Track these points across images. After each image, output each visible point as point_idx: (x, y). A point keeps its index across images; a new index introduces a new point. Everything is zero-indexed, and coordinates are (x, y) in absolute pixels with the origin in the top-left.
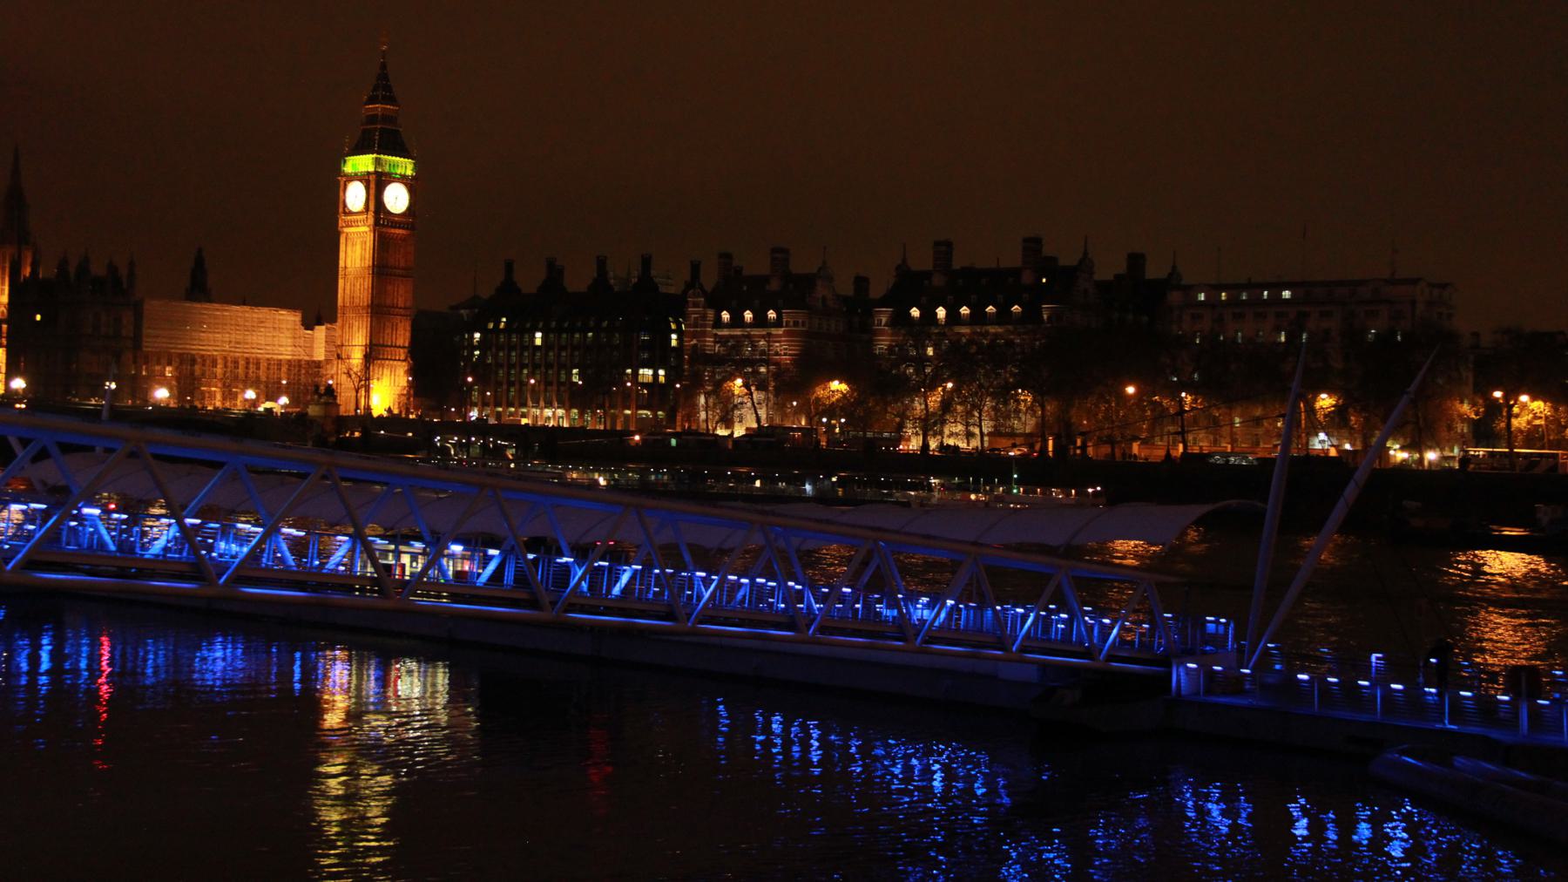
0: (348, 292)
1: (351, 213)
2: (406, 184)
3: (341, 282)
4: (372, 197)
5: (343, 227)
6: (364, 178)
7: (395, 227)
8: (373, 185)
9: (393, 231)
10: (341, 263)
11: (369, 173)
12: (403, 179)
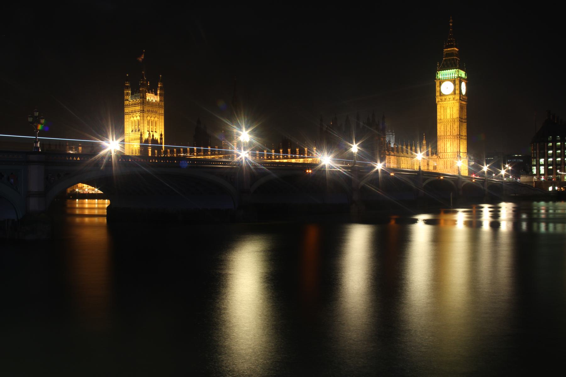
1: (444, 95)
3: (438, 126)
8: (457, 82)
10: (438, 117)
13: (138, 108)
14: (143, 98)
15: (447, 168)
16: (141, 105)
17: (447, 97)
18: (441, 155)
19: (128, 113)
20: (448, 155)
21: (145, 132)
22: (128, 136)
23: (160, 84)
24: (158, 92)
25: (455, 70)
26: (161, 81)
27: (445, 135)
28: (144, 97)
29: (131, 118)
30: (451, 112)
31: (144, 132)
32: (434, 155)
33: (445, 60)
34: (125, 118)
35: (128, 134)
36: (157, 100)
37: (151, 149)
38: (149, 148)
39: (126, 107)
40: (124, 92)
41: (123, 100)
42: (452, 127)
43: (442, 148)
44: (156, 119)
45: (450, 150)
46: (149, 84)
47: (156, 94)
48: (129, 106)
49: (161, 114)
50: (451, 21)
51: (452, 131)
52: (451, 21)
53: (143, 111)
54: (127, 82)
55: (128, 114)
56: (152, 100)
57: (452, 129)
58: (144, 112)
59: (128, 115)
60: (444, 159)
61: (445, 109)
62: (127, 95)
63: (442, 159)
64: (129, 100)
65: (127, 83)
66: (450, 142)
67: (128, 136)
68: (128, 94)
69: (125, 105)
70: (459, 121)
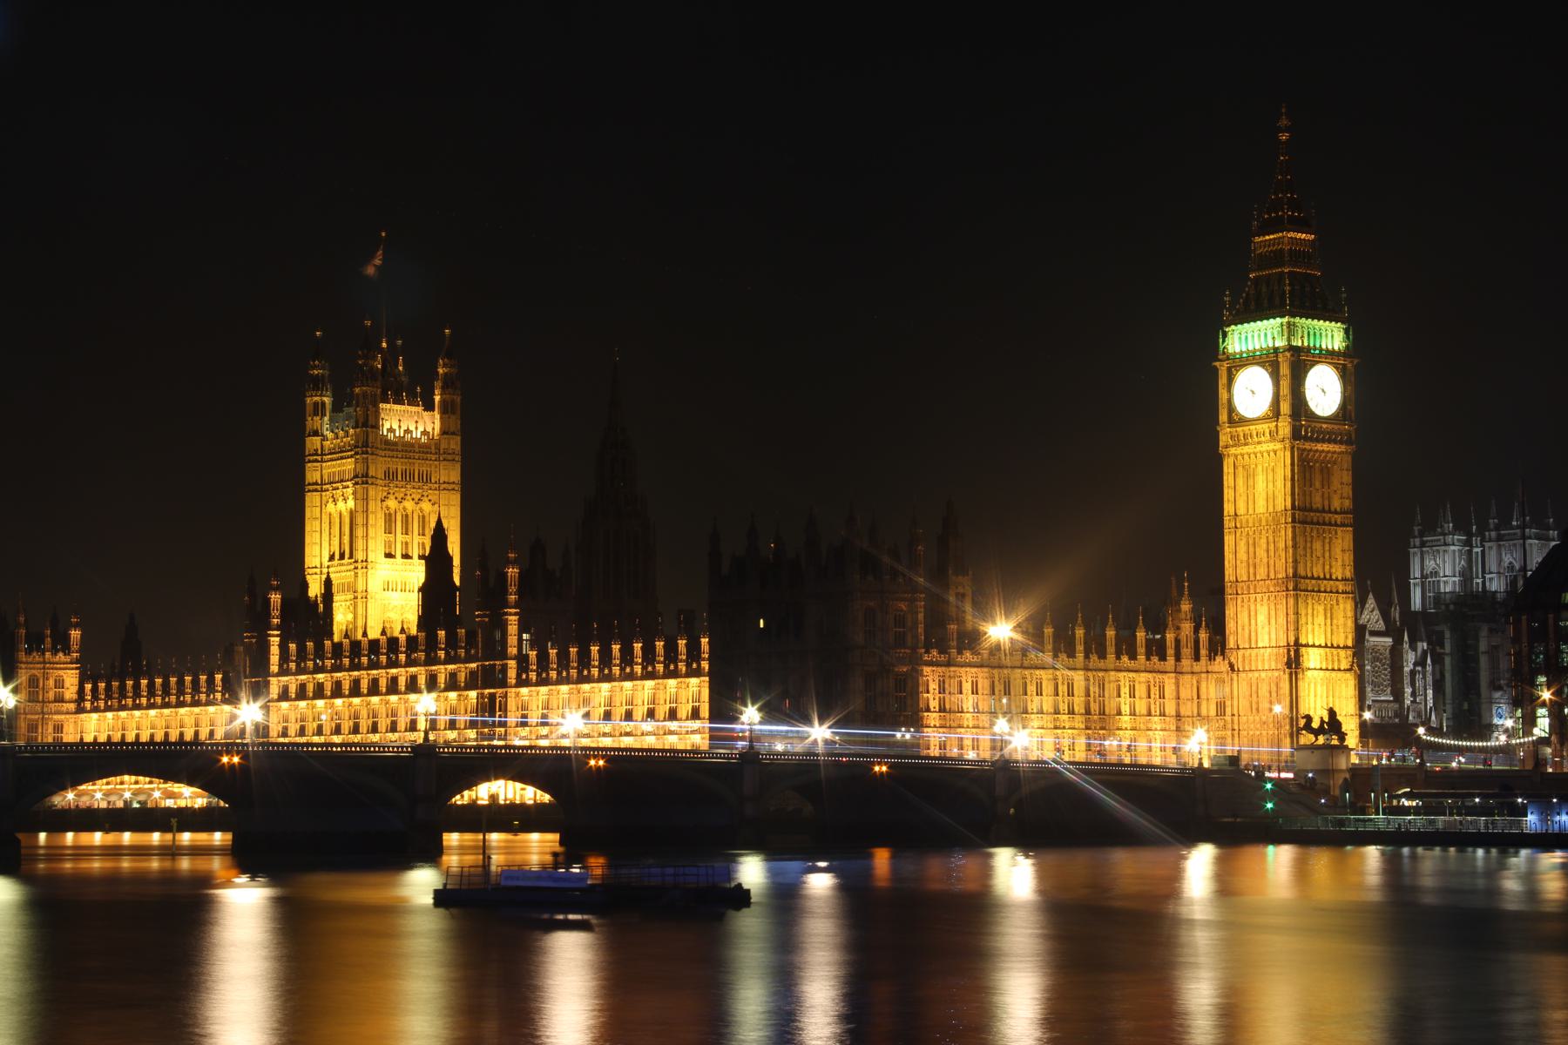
0: (1242, 555)
1: (1243, 421)
2: (1336, 366)
3: (1229, 540)
6: (1269, 360)
7: (1323, 441)
8: (1285, 370)
9: (1320, 447)
10: (1228, 508)
13: (348, 465)
14: (365, 425)
15: (1258, 710)
16: (357, 453)
17: (1252, 427)
18: (1237, 658)
19: (316, 484)
20: (1260, 658)
21: (369, 560)
22: (318, 577)
23: (445, 365)
24: (437, 398)
25: (1279, 320)
26: (449, 355)
27: (1252, 578)
28: (369, 423)
29: (328, 505)
30: (1271, 485)
31: (366, 561)
32: (1219, 659)
33: (1257, 280)
34: (307, 504)
35: (314, 570)
36: (429, 429)
37: (278, 639)
38: (507, 614)
39: (310, 461)
40: (305, 402)
41: (299, 433)
42: (1272, 547)
43: (1243, 629)
45: (1266, 637)
46: (401, 368)
47: (429, 407)
48: (321, 455)
49: (445, 486)
50: (1284, 122)
51: (1272, 562)
52: (1284, 122)
53: (362, 478)
54: (317, 362)
55: (319, 487)
56: (408, 431)
57: (1272, 553)
58: (367, 483)
59: (316, 490)
60: (1250, 675)
61: (1250, 475)
62: (316, 414)
63: (1242, 675)
64: (326, 432)
65: (315, 367)
66: (1265, 608)
67: (314, 576)
68: (319, 409)
69: (307, 453)
70: (1293, 521)
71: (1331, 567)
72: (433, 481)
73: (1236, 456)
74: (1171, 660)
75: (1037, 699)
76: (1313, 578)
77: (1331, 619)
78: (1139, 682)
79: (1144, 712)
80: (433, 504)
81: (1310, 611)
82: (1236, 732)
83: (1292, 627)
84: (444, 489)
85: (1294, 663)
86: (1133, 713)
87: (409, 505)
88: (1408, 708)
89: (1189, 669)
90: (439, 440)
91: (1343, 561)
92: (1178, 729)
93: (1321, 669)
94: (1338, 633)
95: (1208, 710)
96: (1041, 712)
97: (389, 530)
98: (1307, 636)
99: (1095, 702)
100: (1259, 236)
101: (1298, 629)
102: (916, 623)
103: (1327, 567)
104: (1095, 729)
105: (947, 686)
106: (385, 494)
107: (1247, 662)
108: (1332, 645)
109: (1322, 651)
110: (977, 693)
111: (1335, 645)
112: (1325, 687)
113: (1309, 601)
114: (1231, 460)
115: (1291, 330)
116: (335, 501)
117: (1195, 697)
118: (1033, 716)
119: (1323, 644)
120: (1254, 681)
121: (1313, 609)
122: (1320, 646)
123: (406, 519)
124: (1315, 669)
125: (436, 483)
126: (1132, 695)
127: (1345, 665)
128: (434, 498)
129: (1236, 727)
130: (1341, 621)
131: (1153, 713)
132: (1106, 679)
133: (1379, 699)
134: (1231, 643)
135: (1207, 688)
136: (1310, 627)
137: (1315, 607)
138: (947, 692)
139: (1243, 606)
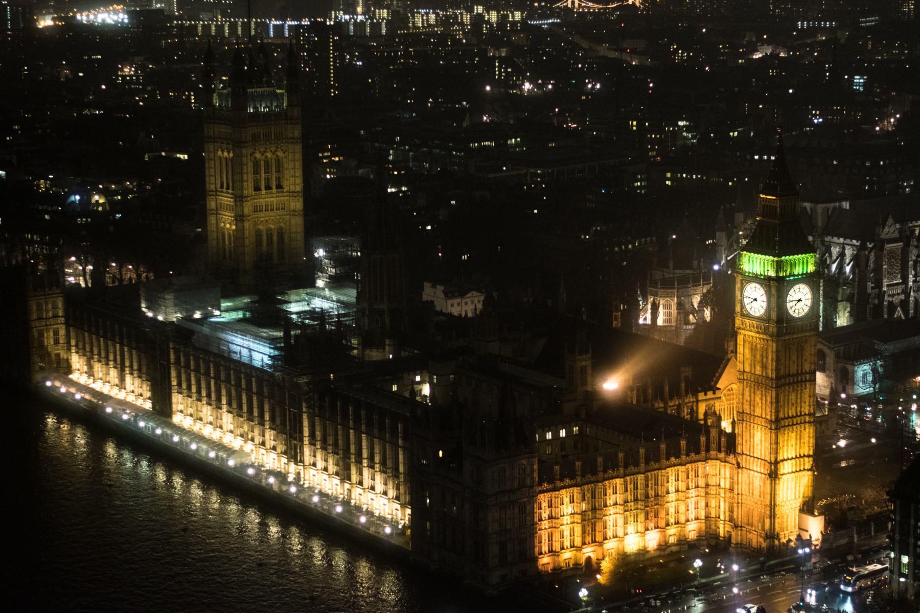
1: (749, 316)
4: (774, 305)
5: (739, 328)
6: (765, 281)
8: (774, 291)
11: (769, 279)
12: (808, 279)
15: (753, 493)
22: (214, 197)
25: (771, 258)
32: (732, 456)
35: (212, 193)
43: (746, 442)
44: (280, 154)
71: (801, 407)
72: (284, 137)
73: (745, 335)
74: (703, 454)
75: (613, 497)
76: (789, 417)
77: (800, 439)
78: (682, 472)
79: (684, 489)
80: (284, 153)
81: (786, 438)
82: (740, 505)
83: (773, 452)
84: (291, 143)
85: (774, 476)
86: (677, 491)
87: (269, 155)
88: (911, 287)
89: (715, 456)
90: (287, 109)
91: (809, 402)
92: (707, 493)
93: (792, 472)
94: (804, 447)
95: (725, 485)
96: (616, 504)
97: (256, 172)
98: (783, 454)
99: (652, 489)
100: (763, 194)
101: (777, 453)
102: (532, 471)
103: (799, 408)
104: (652, 506)
105: (553, 502)
106: (253, 150)
107: (747, 463)
108: (800, 455)
109: (793, 461)
110: (573, 502)
111: (802, 455)
112: (794, 483)
113: (786, 433)
114: (742, 337)
115: (779, 266)
116: (223, 151)
117: (718, 474)
118: (610, 508)
119: (794, 457)
120: (751, 476)
121: (788, 436)
122: (792, 458)
123: (267, 163)
124: (789, 473)
125: (286, 138)
126: (677, 480)
127: (808, 466)
128: (284, 148)
129: (740, 501)
130: (807, 439)
131: (690, 487)
132: (660, 474)
133: (892, 283)
134: (739, 451)
135: (725, 471)
136: (785, 448)
137: (790, 435)
138: (553, 506)
139: (746, 428)
